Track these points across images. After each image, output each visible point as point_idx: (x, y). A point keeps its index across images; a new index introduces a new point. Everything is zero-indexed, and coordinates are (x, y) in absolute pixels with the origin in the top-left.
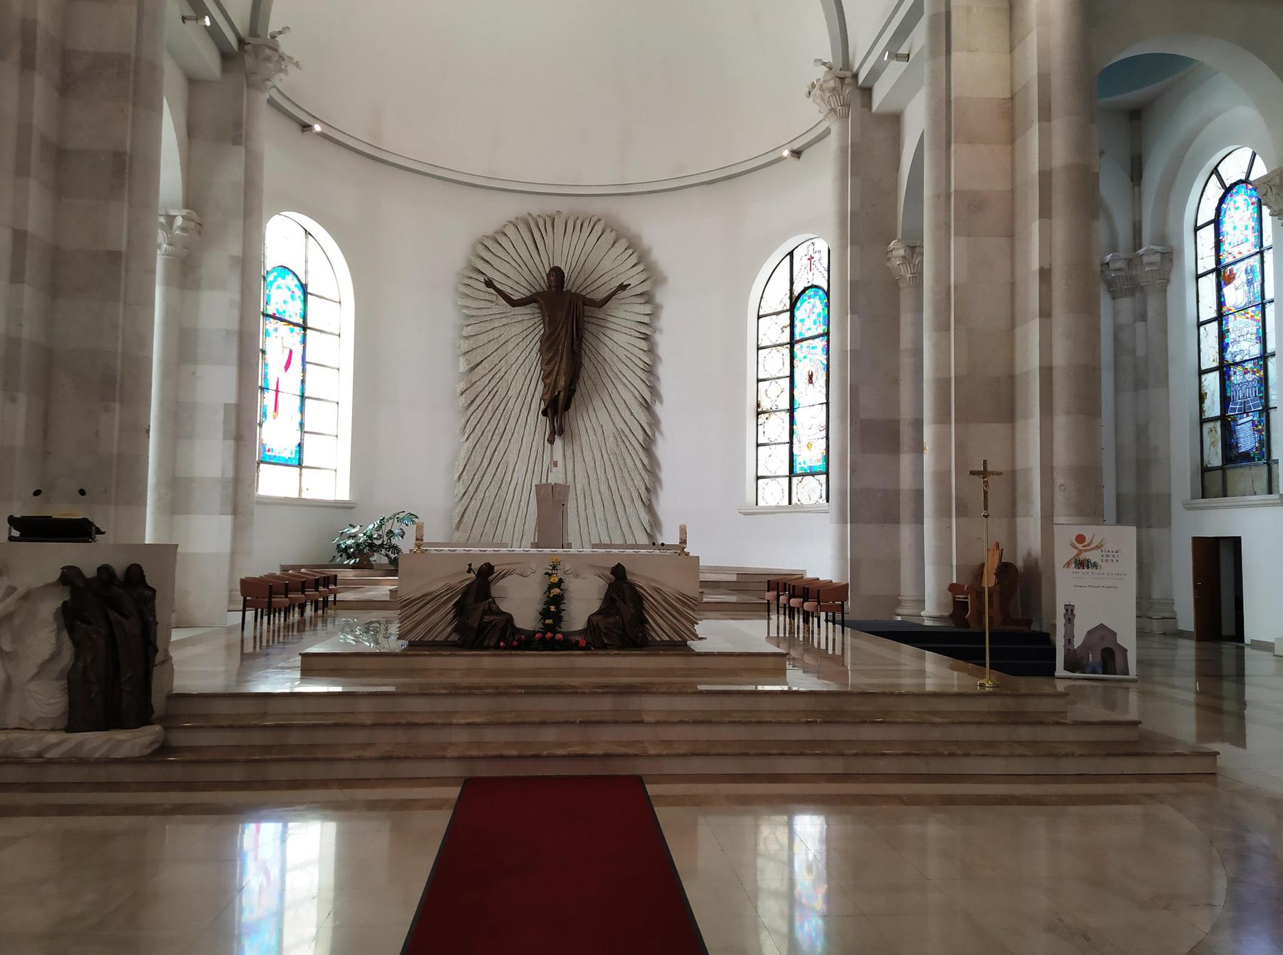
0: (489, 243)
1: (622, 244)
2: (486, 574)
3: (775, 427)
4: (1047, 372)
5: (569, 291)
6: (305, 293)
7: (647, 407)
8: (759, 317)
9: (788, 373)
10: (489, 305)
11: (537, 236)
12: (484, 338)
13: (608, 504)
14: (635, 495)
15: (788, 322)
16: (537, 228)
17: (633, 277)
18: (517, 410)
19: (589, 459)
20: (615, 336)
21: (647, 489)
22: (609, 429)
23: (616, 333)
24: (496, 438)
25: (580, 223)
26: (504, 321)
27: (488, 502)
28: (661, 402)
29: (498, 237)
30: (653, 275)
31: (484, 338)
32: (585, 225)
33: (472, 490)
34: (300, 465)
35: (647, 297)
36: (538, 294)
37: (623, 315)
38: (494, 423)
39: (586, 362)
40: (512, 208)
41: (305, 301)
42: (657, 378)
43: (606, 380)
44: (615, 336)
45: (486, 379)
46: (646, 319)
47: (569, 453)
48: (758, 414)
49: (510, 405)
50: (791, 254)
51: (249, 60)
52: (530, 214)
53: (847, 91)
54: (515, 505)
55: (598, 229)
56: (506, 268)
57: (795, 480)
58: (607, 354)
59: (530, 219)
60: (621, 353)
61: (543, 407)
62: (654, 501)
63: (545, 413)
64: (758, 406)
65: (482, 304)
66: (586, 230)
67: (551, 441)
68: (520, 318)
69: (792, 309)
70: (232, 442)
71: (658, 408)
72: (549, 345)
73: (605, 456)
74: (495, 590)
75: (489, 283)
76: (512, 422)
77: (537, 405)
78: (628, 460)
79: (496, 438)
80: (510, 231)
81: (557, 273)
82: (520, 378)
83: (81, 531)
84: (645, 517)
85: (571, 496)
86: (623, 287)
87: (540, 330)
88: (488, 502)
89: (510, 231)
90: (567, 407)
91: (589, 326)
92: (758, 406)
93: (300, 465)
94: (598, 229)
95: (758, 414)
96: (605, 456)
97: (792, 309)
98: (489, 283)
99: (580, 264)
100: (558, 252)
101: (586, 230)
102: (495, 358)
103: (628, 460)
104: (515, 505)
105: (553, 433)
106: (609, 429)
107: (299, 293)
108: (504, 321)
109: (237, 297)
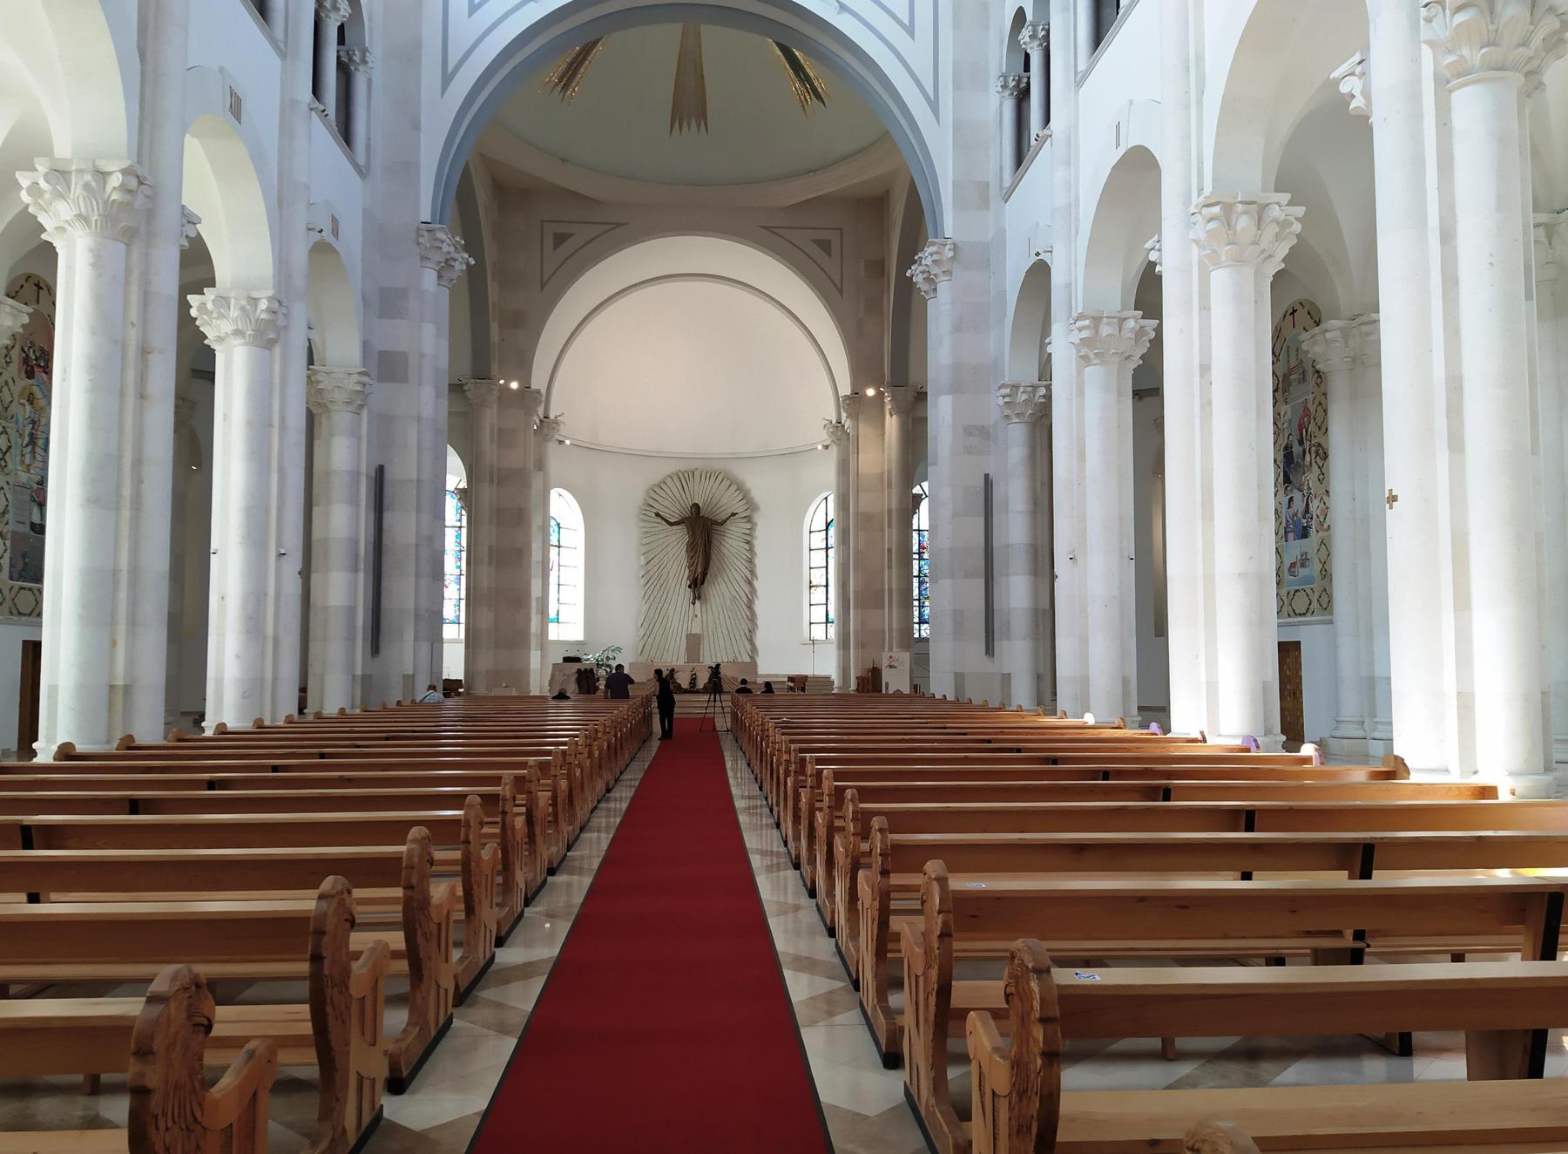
0: (657, 490)
1: (734, 487)
2: (673, 670)
3: (818, 596)
4: (890, 590)
5: (703, 516)
6: (559, 528)
7: (750, 583)
8: (811, 532)
9: (825, 565)
10: (657, 525)
11: (684, 483)
12: (655, 545)
13: (727, 639)
14: (743, 634)
15: (825, 537)
16: (684, 477)
17: (739, 508)
18: (674, 585)
19: (716, 613)
20: (730, 541)
21: (750, 631)
22: (727, 596)
23: (733, 541)
24: (662, 602)
25: (709, 474)
26: (666, 534)
27: (658, 639)
28: (757, 579)
29: (661, 485)
30: (752, 506)
31: (655, 545)
32: (712, 476)
33: (648, 632)
34: (558, 622)
35: (749, 519)
36: (686, 518)
37: (734, 529)
38: (661, 593)
39: (713, 557)
40: (671, 468)
41: (559, 532)
42: (755, 566)
43: (725, 567)
44: (730, 541)
45: (656, 569)
46: (748, 532)
47: (704, 610)
48: (811, 587)
49: (670, 582)
50: (826, 498)
51: (545, 429)
52: (680, 471)
53: (839, 433)
54: (673, 642)
55: (720, 478)
56: (666, 503)
57: (829, 625)
58: (725, 551)
59: (680, 474)
60: (733, 550)
61: (688, 583)
62: (753, 636)
63: (690, 587)
64: (811, 582)
65: (653, 525)
66: (713, 479)
67: (694, 604)
68: (674, 532)
69: (827, 530)
70: (540, 616)
71: (756, 583)
72: (691, 547)
73: (725, 612)
74: (675, 676)
75: (657, 515)
76: (671, 592)
77: (686, 582)
78: (739, 614)
79: (662, 602)
80: (669, 481)
81: (696, 506)
82: (675, 566)
83: (577, 660)
84: (748, 647)
85: (706, 640)
86: (734, 514)
87: (687, 538)
88: (658, 639)
89: (669, 481)
90: (702, 583)
91: (715, 536)
92: (811, 582)
93: (558, 622)
94: (720, 478)
95: (811, 587)
96: (725, 612)
97: (827, 530)
98: (657, 515)
99: (709, 499)
100: (696, 494)
101: (713, 479)
102: (661, 555)
103: (739, 614)
104: (673, 642)
105: (695, 598)
106: (727, 596)
107: (556, 528)
108: (666, 534)
109: (541, 545)
